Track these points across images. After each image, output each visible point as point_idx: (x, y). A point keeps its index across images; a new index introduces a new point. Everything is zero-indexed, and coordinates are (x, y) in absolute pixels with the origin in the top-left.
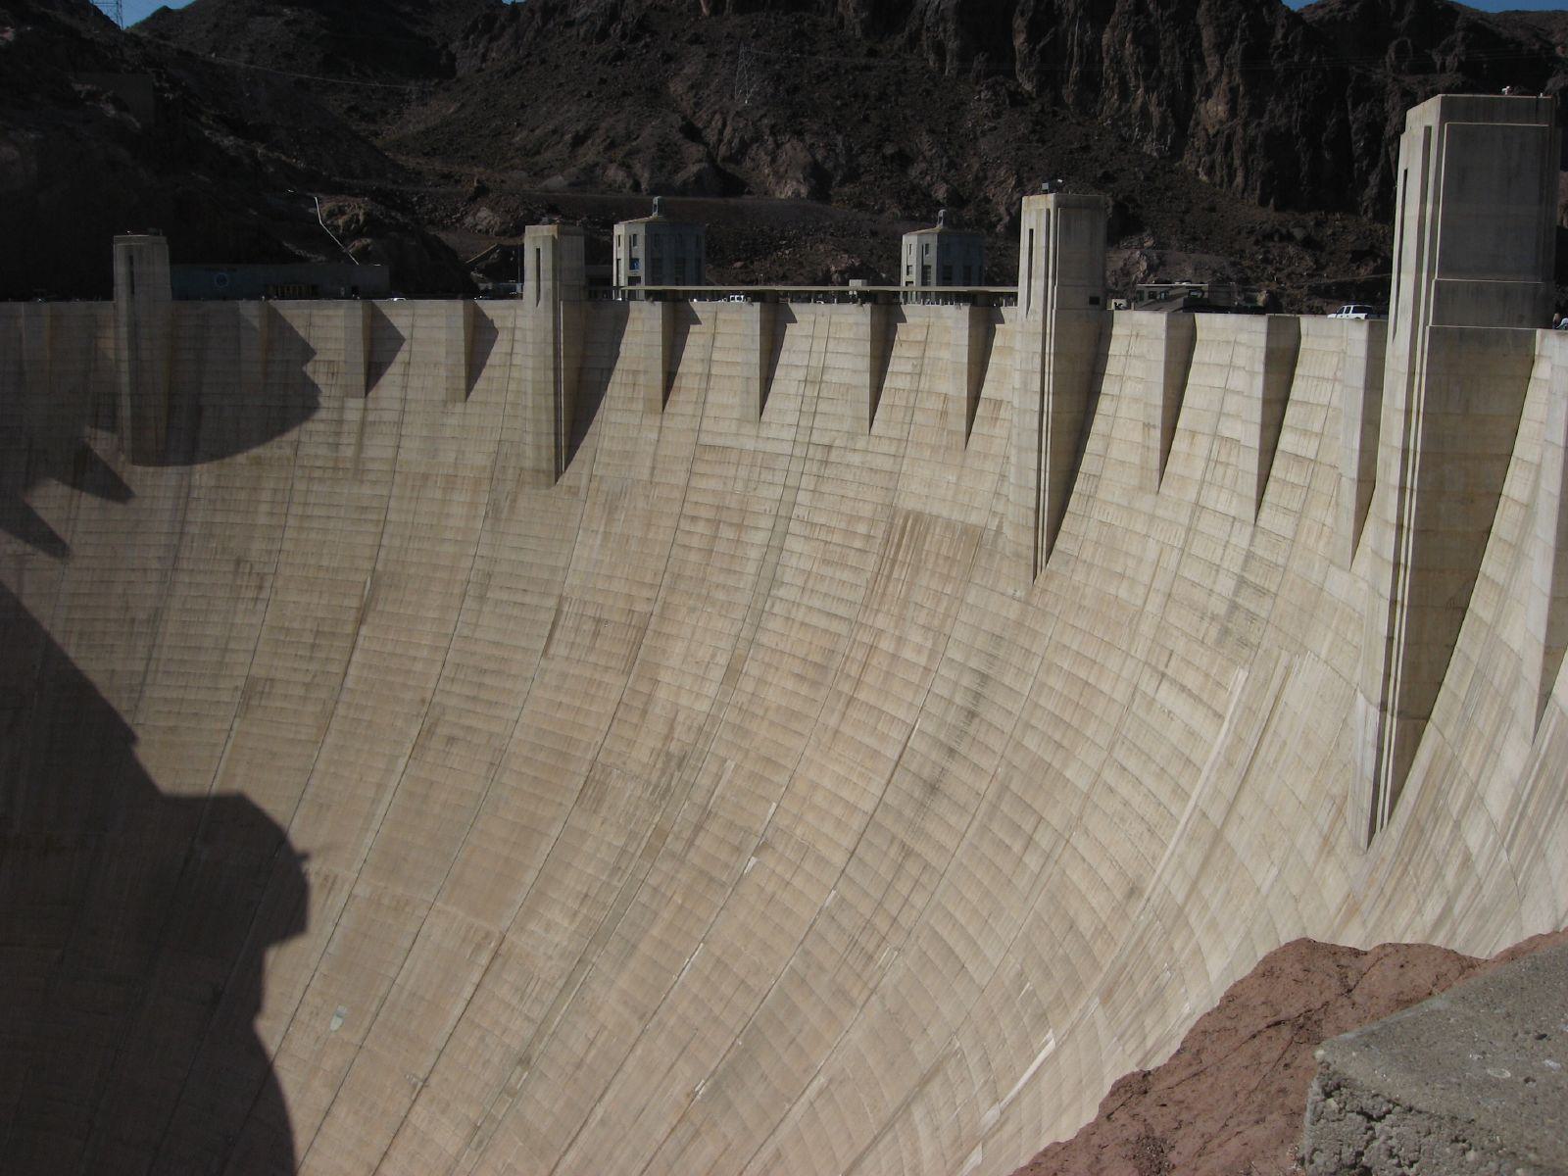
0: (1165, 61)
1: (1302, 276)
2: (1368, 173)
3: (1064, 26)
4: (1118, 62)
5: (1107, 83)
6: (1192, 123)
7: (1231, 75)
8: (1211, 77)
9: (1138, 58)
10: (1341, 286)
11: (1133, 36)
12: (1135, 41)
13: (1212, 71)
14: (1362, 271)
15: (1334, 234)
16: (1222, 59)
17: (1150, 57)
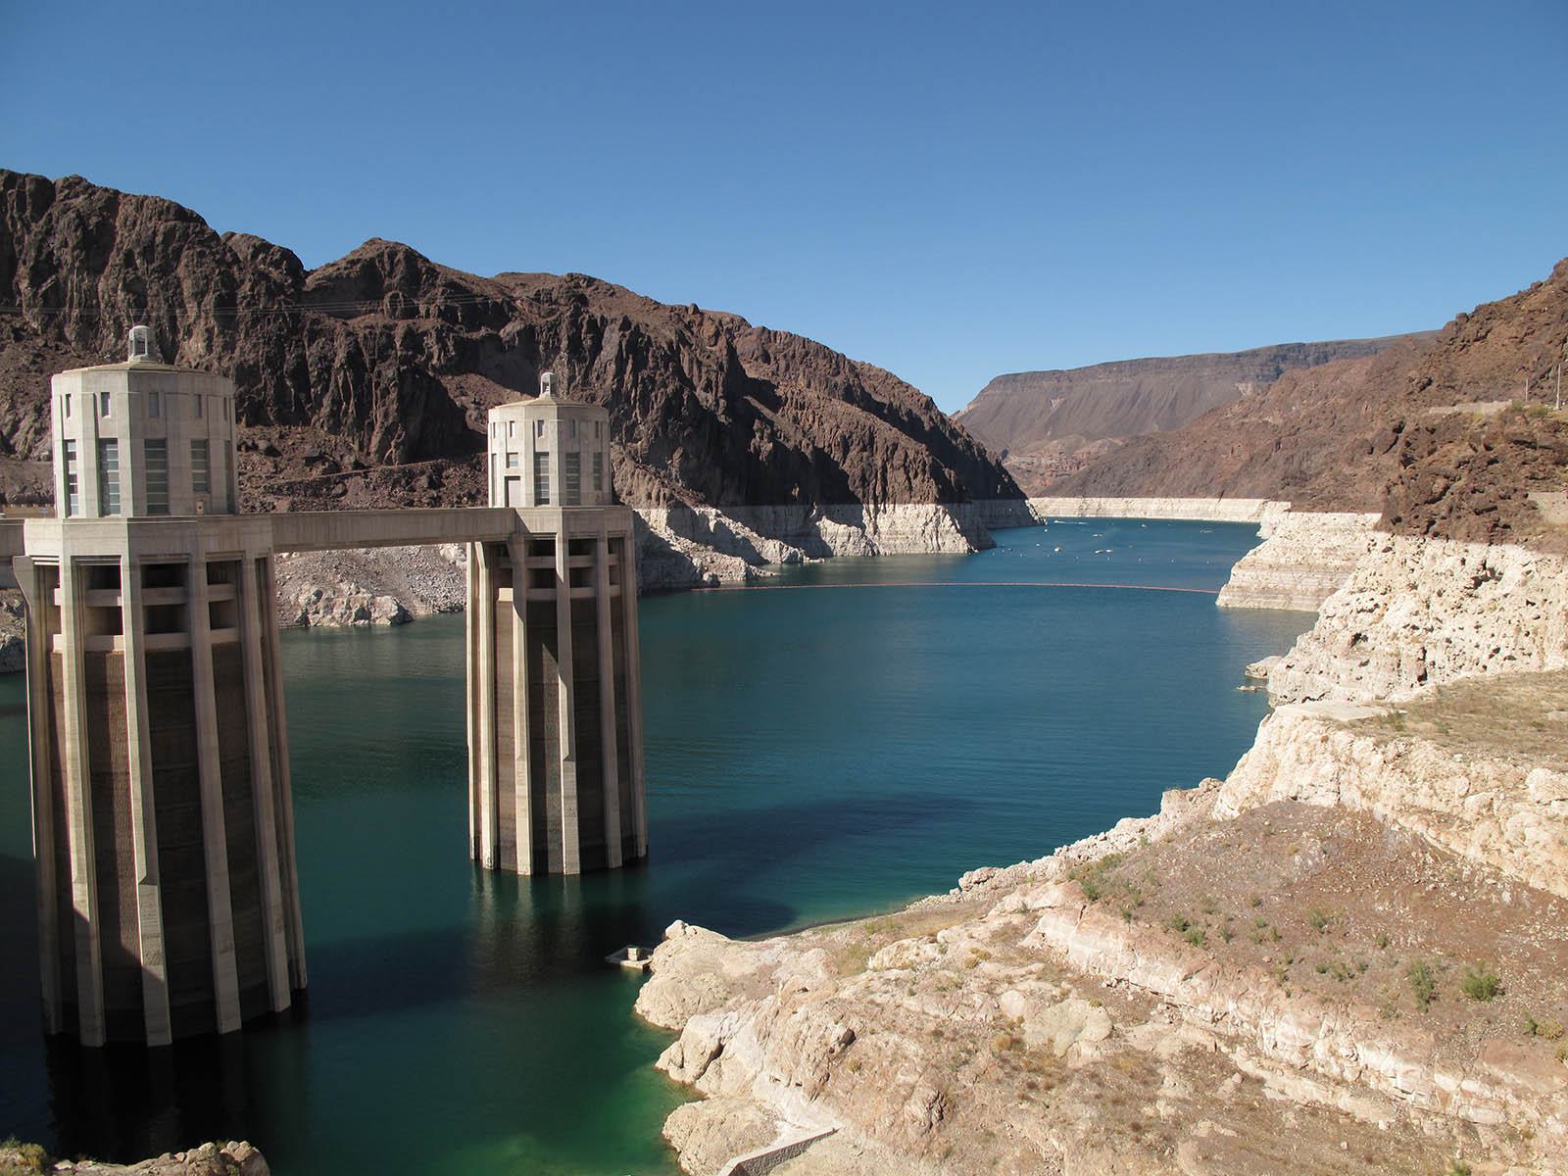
0: (152, 307)
1: (261, 477)
2: (322, 395)
3: (64, 275)
4: (113, 306)
5: (104, 324)
6: (177, 357)
7: (207, 318)
8: (191, 320)
9: (129, 302)
10: (291, 485)
11: (124, 285)
12: (127, 288)
13: (192, 314)
14: (314, 472)
15: (293, 444)
16: (199, 307)
17: (140, 302)
